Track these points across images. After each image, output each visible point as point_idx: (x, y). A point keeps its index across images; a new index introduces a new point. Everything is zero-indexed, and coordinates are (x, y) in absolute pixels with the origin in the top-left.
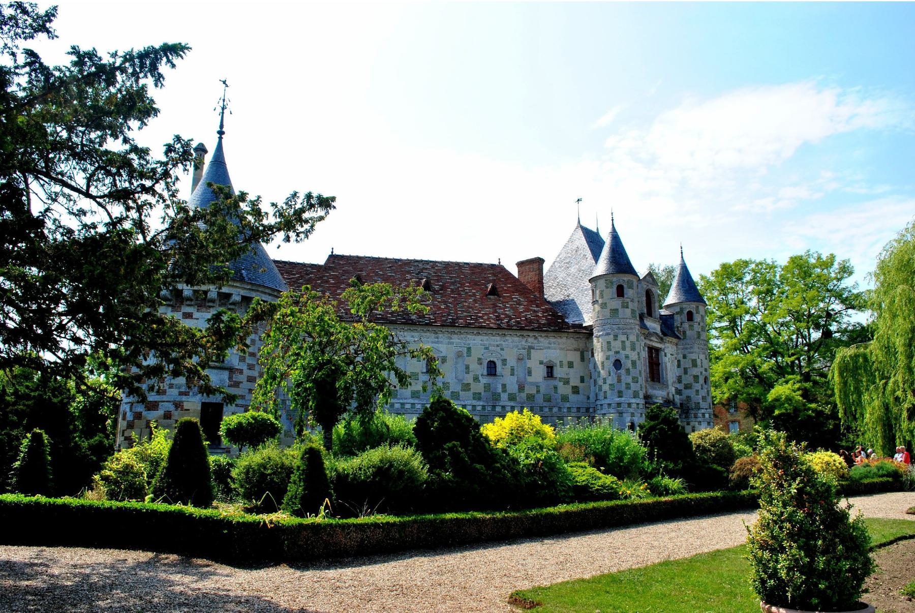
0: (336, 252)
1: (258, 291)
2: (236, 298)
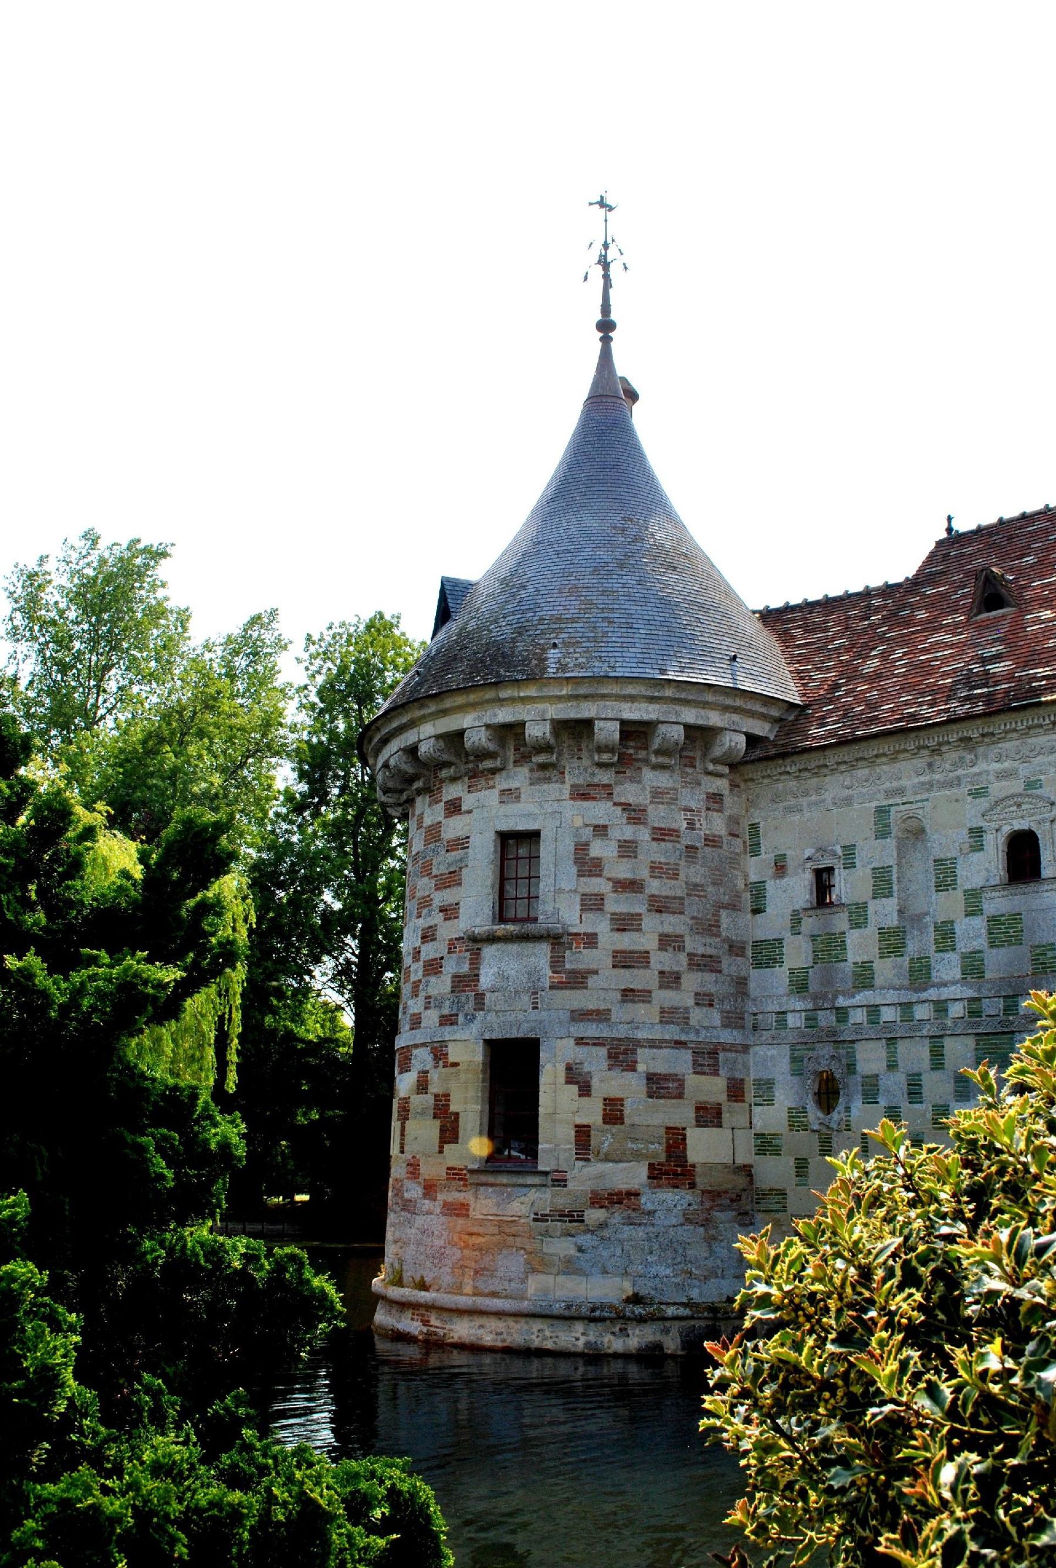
0: (963, 525)
1: (604, 696)
2: (537, 731)
